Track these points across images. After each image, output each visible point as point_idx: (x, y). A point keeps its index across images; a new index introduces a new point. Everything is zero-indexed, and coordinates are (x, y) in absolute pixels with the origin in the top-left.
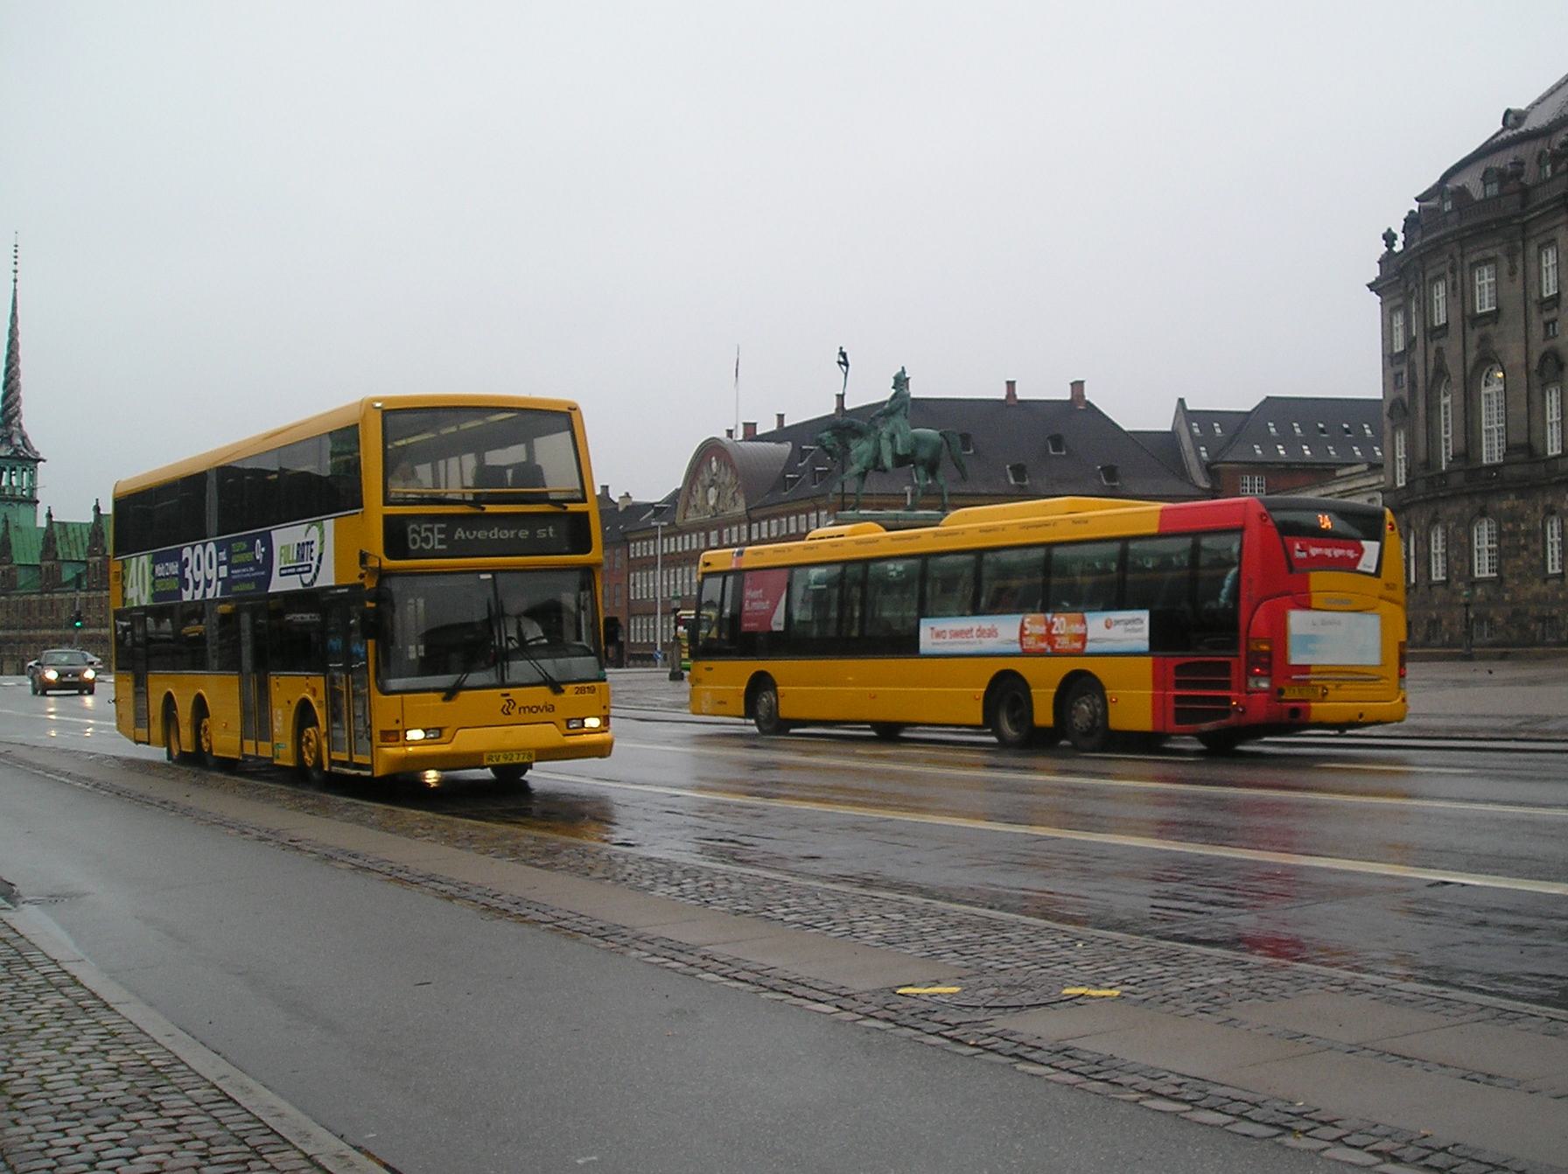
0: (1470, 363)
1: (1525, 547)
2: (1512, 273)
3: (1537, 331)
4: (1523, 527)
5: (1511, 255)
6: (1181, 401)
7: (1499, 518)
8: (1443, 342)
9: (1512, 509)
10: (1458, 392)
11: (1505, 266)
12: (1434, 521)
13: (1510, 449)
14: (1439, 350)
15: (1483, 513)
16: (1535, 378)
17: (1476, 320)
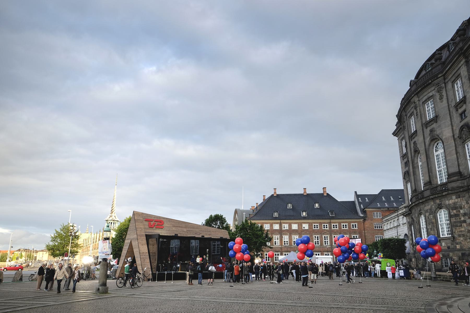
0: (427, 143)
1: (465, 221)
2: (441, 98)
3: (456, 119)
4: (462, 211)
5: (439, 91)
6: (356, 192)
7: (448, 208)
8: (416, 139)
9: (454, 203)
10: (424, 159)
11: (438, 97)
12: (420, 214)
13: (450, 176)
14: (415, 143)
15: (440, 207)
16: (459, 141)
17: (427, 124)
